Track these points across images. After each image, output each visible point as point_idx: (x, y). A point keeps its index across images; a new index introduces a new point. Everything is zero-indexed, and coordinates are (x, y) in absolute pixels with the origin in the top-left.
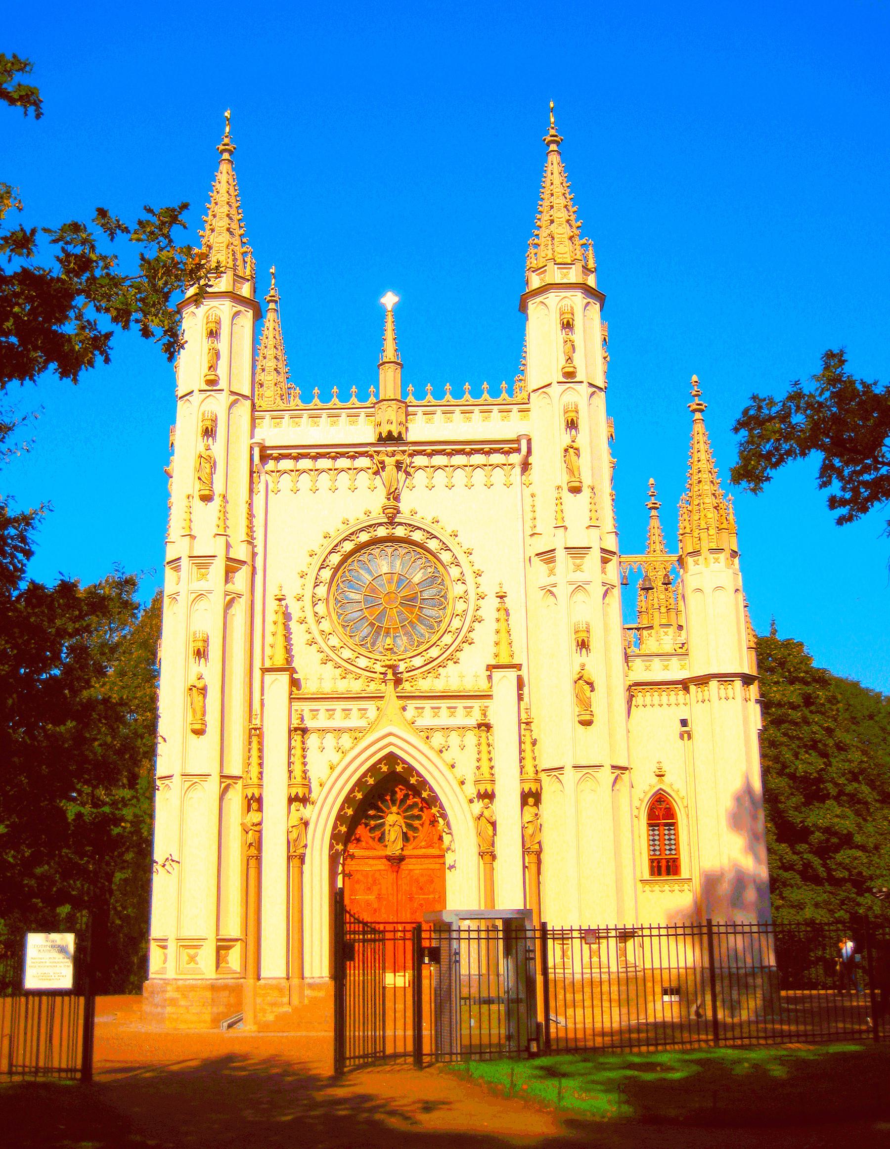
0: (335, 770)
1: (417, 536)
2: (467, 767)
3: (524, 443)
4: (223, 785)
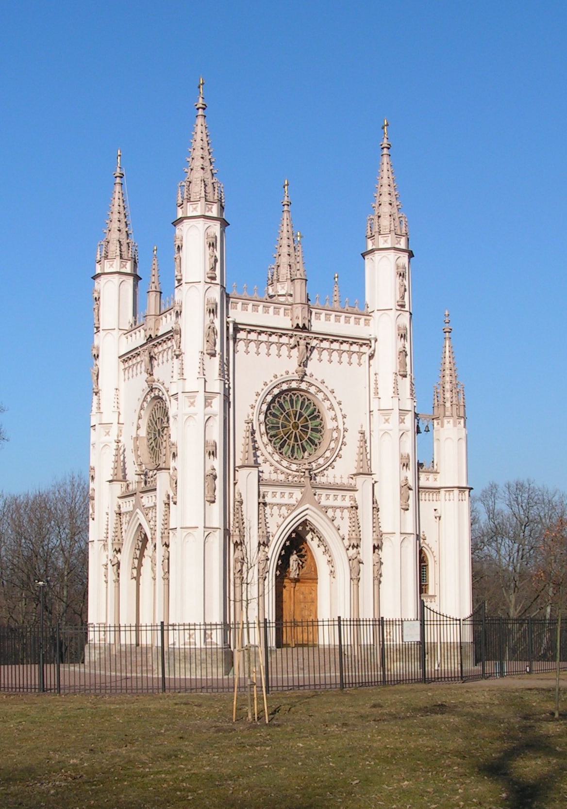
0: (279, 530)
1: (312, 390)
4: (206, 534)
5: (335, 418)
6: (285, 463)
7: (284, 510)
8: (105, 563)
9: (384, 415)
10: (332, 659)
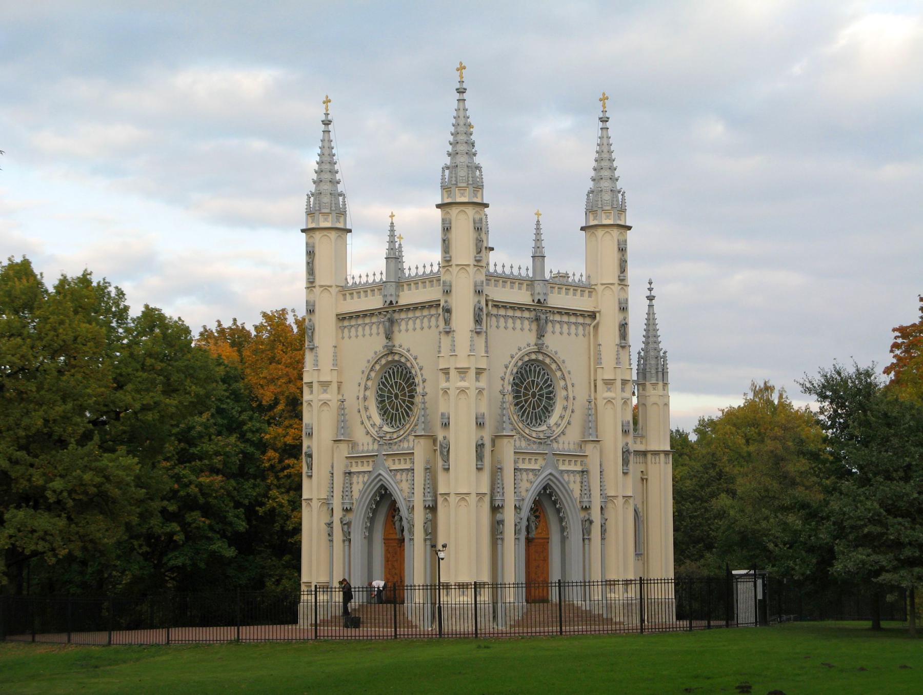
1: (548, 361)
2: (577, 493)
3: (597, 315)
5: (566, 388)
6: (527, 431)
7: (531, 476)
8: (328, 521)
9: (606, 384)
10: (483, 619)
